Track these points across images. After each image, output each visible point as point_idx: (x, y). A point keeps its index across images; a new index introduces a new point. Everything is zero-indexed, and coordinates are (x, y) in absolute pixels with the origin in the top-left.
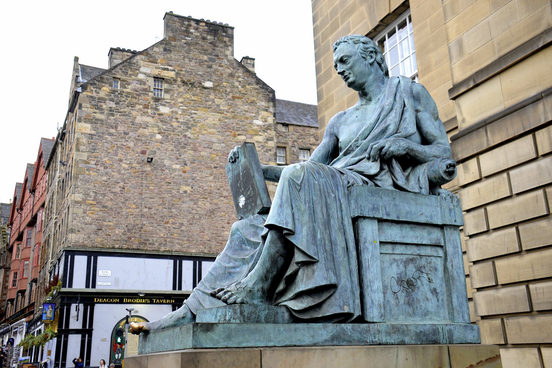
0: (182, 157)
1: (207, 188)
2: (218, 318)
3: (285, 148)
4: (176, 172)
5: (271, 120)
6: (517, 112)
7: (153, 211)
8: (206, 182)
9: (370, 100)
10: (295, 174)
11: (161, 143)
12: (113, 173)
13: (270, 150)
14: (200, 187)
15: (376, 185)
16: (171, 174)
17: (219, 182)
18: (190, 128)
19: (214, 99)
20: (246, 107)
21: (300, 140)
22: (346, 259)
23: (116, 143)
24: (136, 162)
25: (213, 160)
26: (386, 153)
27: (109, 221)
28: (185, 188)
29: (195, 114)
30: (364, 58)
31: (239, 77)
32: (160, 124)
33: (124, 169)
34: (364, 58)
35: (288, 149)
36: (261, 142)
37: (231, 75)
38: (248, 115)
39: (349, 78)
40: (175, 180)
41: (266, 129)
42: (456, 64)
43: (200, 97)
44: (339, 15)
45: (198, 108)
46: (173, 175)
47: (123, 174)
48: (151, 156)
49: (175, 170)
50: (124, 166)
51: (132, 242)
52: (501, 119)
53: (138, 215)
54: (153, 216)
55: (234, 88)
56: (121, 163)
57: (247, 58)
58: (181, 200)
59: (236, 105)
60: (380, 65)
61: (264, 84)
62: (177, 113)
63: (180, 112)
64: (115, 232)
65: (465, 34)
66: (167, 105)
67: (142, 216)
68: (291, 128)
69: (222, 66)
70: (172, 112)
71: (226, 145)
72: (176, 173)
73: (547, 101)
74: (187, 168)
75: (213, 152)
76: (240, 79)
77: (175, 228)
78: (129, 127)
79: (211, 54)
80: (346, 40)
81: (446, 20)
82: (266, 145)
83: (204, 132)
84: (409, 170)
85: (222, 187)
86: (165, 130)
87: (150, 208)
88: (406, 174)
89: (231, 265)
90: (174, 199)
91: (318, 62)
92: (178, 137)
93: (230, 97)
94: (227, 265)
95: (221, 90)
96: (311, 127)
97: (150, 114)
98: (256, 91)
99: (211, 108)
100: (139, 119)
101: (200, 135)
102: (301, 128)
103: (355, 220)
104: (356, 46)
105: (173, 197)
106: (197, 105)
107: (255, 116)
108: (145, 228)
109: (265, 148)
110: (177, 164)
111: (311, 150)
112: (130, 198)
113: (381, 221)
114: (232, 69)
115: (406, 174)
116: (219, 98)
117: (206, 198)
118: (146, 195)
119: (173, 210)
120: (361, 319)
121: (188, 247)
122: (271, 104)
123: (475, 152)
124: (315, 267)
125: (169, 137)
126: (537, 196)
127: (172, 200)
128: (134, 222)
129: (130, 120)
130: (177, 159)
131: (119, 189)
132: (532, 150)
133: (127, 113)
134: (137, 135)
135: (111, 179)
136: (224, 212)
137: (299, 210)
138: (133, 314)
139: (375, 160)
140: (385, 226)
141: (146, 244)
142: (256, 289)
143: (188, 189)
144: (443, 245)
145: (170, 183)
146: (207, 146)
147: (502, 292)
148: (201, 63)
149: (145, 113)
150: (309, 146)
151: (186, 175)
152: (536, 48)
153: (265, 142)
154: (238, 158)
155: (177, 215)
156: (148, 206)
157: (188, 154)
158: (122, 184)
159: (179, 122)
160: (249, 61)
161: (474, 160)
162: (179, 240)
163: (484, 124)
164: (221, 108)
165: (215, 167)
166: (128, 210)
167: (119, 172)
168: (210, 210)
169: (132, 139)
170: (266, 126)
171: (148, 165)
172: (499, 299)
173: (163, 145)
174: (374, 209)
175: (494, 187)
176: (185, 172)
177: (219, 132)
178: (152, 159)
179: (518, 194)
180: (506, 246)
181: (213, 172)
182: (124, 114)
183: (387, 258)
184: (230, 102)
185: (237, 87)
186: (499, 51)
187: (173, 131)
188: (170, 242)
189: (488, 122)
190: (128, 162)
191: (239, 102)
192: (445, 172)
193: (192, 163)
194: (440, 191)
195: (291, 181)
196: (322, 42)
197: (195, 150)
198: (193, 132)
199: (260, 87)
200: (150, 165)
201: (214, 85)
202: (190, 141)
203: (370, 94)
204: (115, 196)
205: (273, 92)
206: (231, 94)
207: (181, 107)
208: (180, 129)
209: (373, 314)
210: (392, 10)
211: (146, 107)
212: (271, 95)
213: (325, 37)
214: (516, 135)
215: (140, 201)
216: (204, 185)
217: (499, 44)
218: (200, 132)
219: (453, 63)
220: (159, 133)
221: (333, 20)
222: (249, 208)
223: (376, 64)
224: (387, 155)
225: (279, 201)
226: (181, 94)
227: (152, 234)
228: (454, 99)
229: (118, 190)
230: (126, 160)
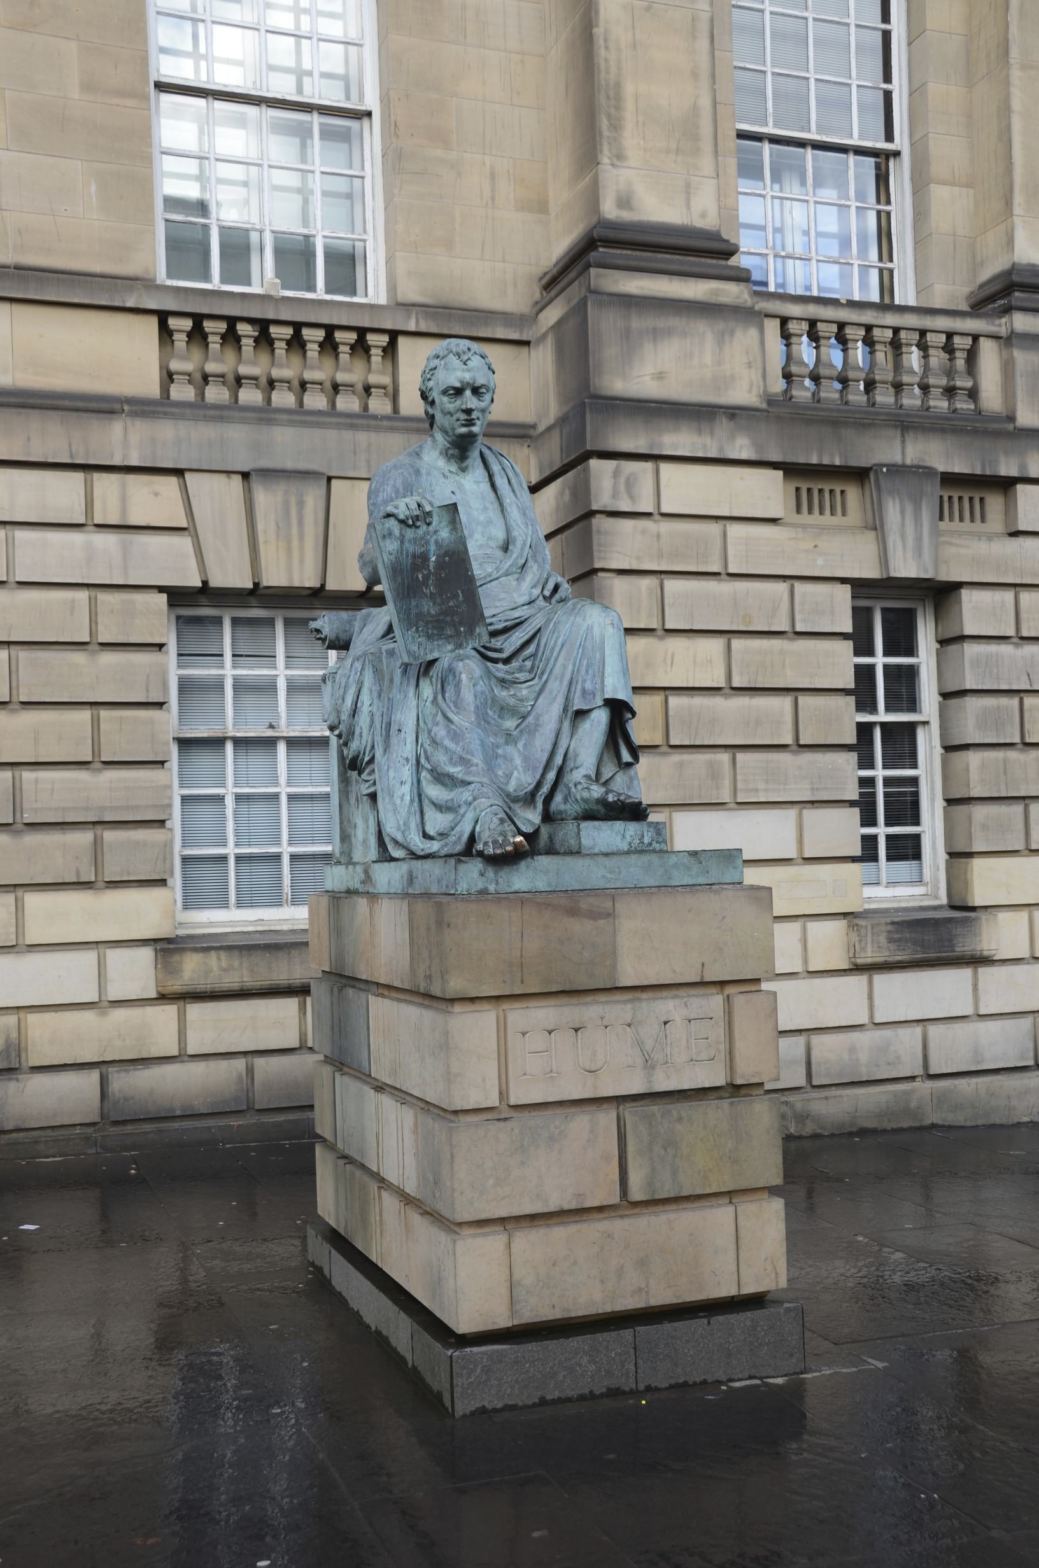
2: (629, 839)
6: (60, 413)
9: (464, 470)
39: (474, 425)
132: (80, 505)
154: (429, 524)
179: (22, 584)
214: (50, 460)
222: (449, 632)
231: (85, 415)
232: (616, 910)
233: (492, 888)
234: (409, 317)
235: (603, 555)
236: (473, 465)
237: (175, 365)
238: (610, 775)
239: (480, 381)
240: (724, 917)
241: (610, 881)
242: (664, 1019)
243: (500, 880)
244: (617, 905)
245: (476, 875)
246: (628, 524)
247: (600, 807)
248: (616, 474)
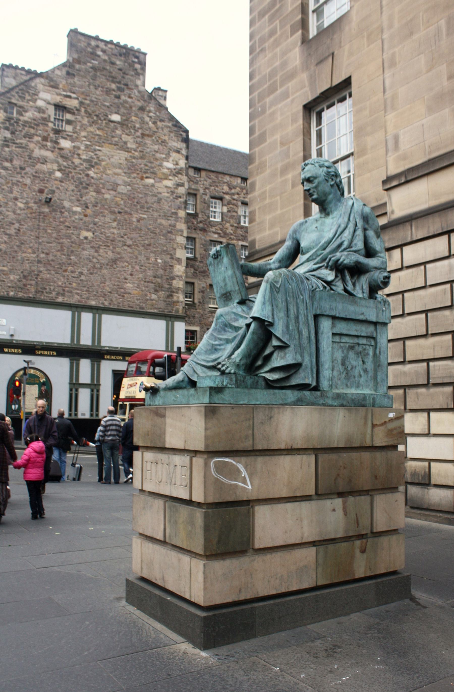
0: (84, 199)
1: (109, 235)
2: (217, 383)
3: (195, 195)
4: (76, 215)
5: (182, 163)
7: (51, 257)
8: (109, 228)
9: (328, 214)
10: (275, 279)
11: (61, 181)
12: (8, 213)
13: (180, 197)
14: (102, 233)
15: (332, 289)
16: (70, 217)
17: (123, 229)
18: (93, 167)
19: (121, 135)
20: (156, 147)
21: (213, 188)
22: (308, 345)
23: (11, 178)
24: (33, 201)
25: (118, 205)
26: (340, 265)
27: (4, 266)
28: (85, 234)
29: (99, 150)
30: (326, 180)
31: (150, 111)
32: (60, 160)
33: (20, 209)
34: (326, 180)
35: (198, 197)
36: (170, 188)
37: (142, 109)
38: (158, 155)
39: (313, 195)
40: (76, 224)
41: (178, 172)
42: (391, 158)
43: (105, 132)
44: (278, 77)
45: (103, 144)
46: (73, 219)
47: (19, 214)
48: (50, 196)
49: (75, 213)
50: (22, 205)
51: (28, 290)
53: (35, 261)
54: (51, 262)
55: (143, 123)
56: (16, 202)
57: (159, 89)
58: (81, 247)
59: (146, 144)
60: (338, 186)
61: (177, 122)
62: (79, 148)
63: (83, 148)
64: (9, 278)
65: (402, 131)
66: (68, 138)
67: (39, 262)
68: (203, 174)
69: (131, 98)
70: (74, 147)
71: (132, 189)
72: (77, 217)
74: (89, 212)
75: (118, 195)
76: (151, 114)
77: (74, 277)
78: (25, 161)
79: (119, 83)
80: (313, 163)
81: (385, 112)
82: (176, 191)
83: (109, 172)
84: (355, 278)
85: (125, 235)
86: (65, 167)
87: (47, 254)
88: (354, 281)
89: (217, 343)
90: (74, 245)
91: (252, 123)
92: (79, 176)
93: (139, 134)
94: (214, 343)
95: (129, 125)
96: (226, 174)
97: (49, 147)
98: (169, 129)
99: (117, 145)
100: (38, 152)
101: (104, 176)
102: (215, 174)
103: (316, 317)
104: (321, 169)
105: (72, 242)
106: (102, 141)
107: (165, 158)
108: (42, 275)
109: (175, 195)
110: (78, 206)
111: (224, 200)
112: (26, 242)
113: (334, 318)
114: (142, 101)
115: (354, 281)
116: (127, 134)
117: (109, 246)
118: (44, 239)
119: (72, 257)
120: (316, 388)
121: (88, 298)
122: (184, 145)
123: (400, 243)
124: (287, 350)
125: (70, 175)
127: (71, 246)
128: (30, 269)
129: (27, 154)
130: (78, 200)
131: (14, 231)
133: (24, 145)
134: (34, 171)
135: (6, 220)
136: (127, 262)
137: (277, 307)
138: (30, 366)
139: (331, 269)
140: (336, 322)
141: (42, 292)
142: (242, 363)
143: (89, 235)
144: (375, 336)
145: (70, 227)
146: (111, 187)
147: (408, 368)
148: (108, 92)
149: (44, 147)
150: (221, 194)
151: (87, 219)
153: (175, 188)
154: (220, 255)
155: (77, 263)
156: (45, 251)
157: (91, 196)
158: (17, 225)
159: (81, 159)
160: (161, 93)
161: (398, 250)
162: (77, 289)
164: (129, 145)
165: (120, 213)
166: (24, 255)
167: (14, 212)
168: (112, 259)
169: (29, 175)
170: (177, 170)
171: (46, 206)
172: (405, 373)
173: (63, 184)
174: (331, 309)
176: (86, 216)
177: (125, 173)
178: (50, 199)
179: (432, 286)
181: (116, 218)
182: (20, 146)
183: (335, 345)
184: (139, 140)
185: (147, 123)
186: (430, 153)
187: (75, 169)
188: (68, 292)
189: (414, 217)
190: (24, 201)
191: (148, 141)
192: (382, 282)
193: (95, 206)
194: (377, 296)
195: (272, 285)
196: (259, 103)
197: (98, 192)
198: (97, 171)
199: (173, 125)
200: (49, 206)
201: (121, 119)
202: (93, 181)
203: (329, 210)
204: (9, 238)
205: (187, 132)
206: (140, 131)
207: (84, 142)
208: (82, 167)
209: (325, 384)
210: (334, 84)
211: (45, 139)
212: (184, 135)
213: (261, 97)
215: (36, 246)
216: (107, 231)
217: (429, 147)
218: (104, 172)
219: (388, 156)
220: (59, 170)
221: (272, 81)
223: (335, 185)
224: (341, 267)
225: (263, 300)
226: (84, 127)
227: (49, 282)
228: (387, 190)
229: (12, 231)
230: (21, 198)
236: (331, 211)
239: (308, 175)
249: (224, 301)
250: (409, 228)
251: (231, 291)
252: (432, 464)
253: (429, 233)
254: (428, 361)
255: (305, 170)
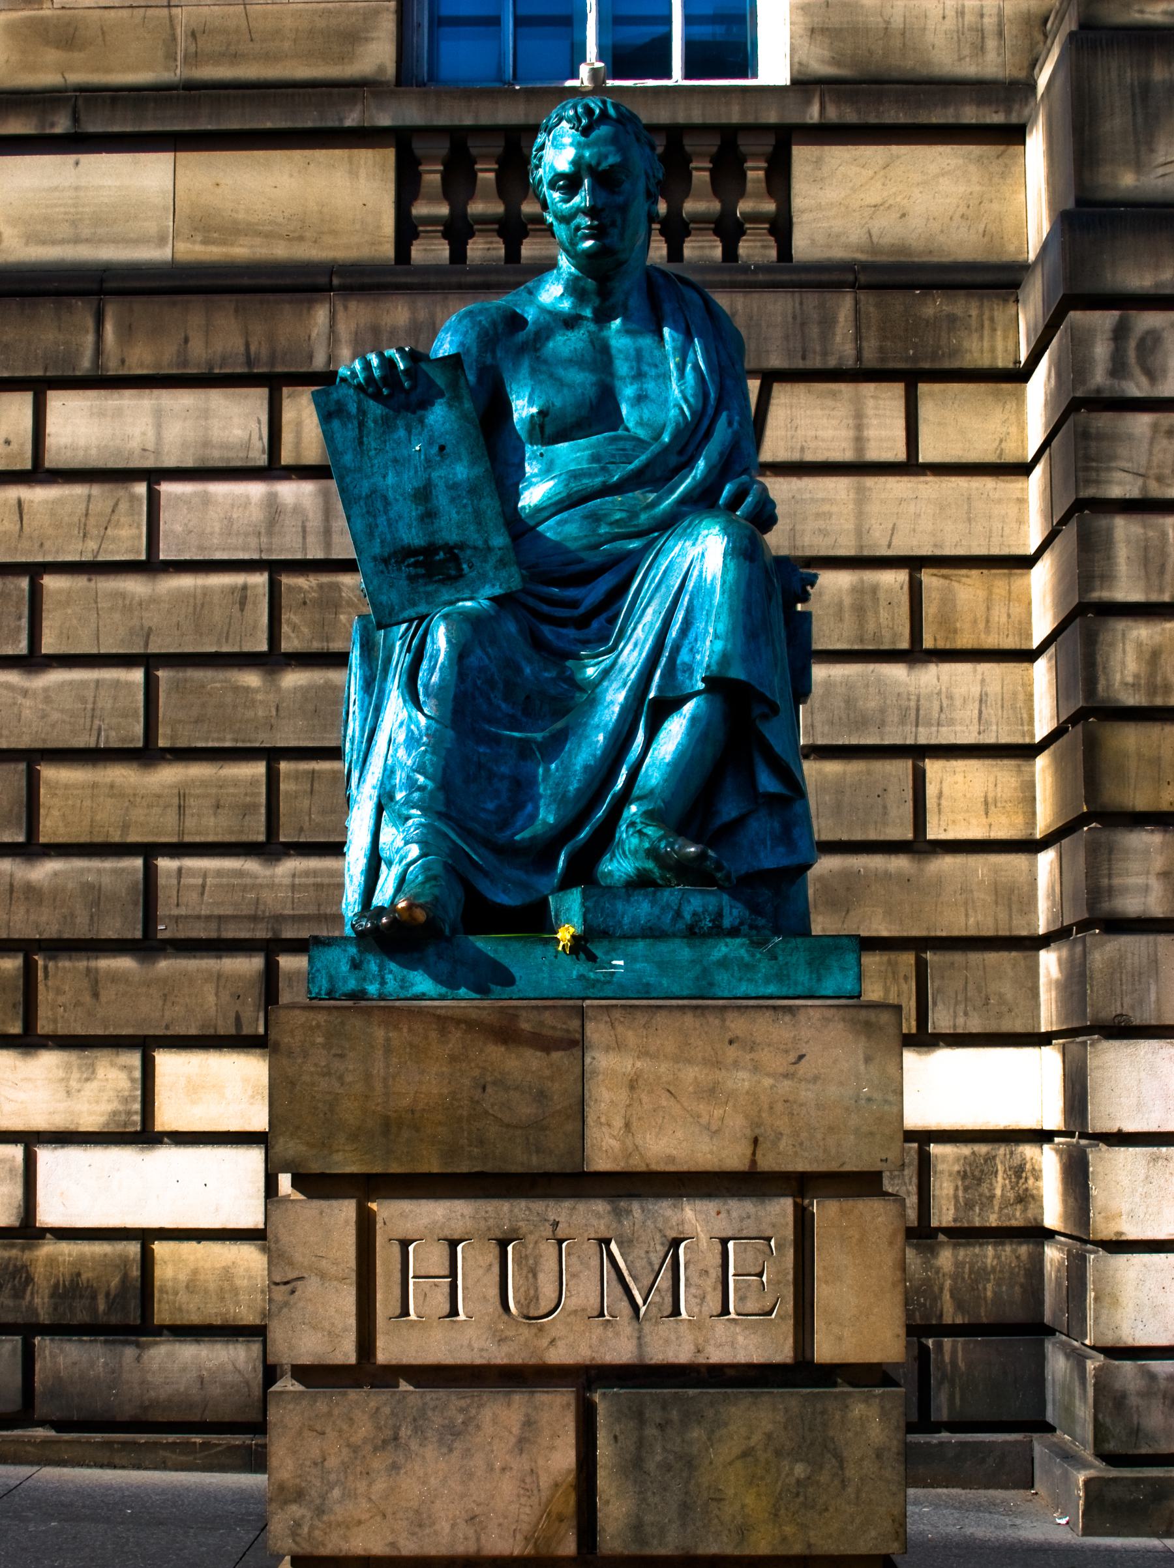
52: (165, 298)
73: (346, 308)
123: (38, 373)
126: (245, 588)
132: (261, 438)
147: (45, 871)
152: (331, 122)
163: (94, 286)
172: (32, 893)
175: (87, 515)
180: (97, 722)
186: (193, 58)
214: (217, 371)
231: (271, 297)
232: (588, 1032)
233: (372, 989)
234: (808, 102)
235: (1094, 475)
237: (420, 209)
238: (734, 814)
240: (801, 1057)
241: (593, 986)
242: (673, 1234)
243: (389, 977)
244: (590, 1027)
245: (344, 968)
246: (1142, 421)
247: (650, 865)
248: (1120, 333)
249: (412, 579)
250: (90, 323)
251: (462, 546)
252: (160, 1248)
253: (185, 364)
254: (149, 851)
255: (594, 135)
